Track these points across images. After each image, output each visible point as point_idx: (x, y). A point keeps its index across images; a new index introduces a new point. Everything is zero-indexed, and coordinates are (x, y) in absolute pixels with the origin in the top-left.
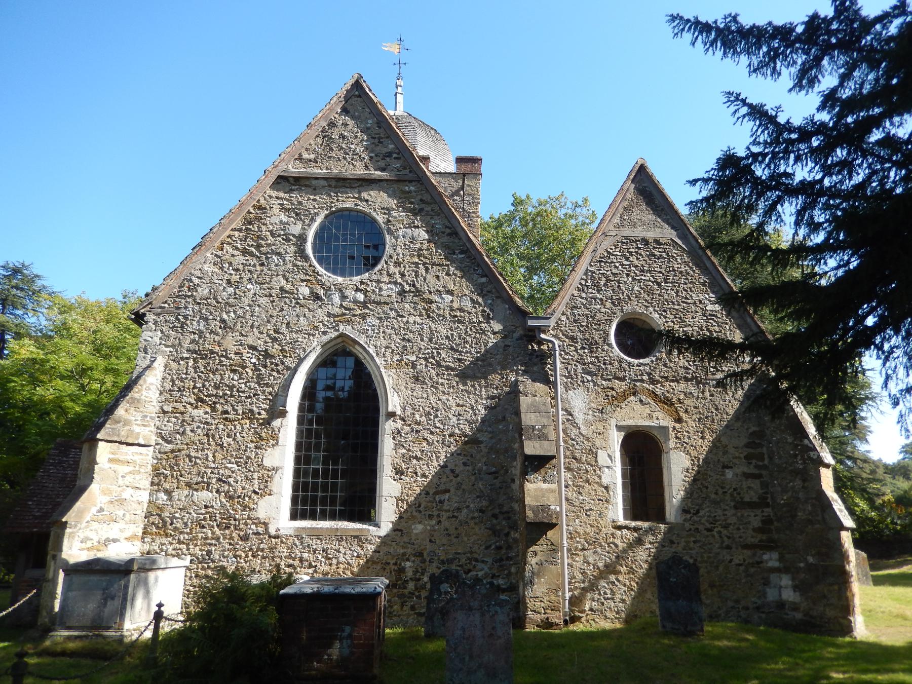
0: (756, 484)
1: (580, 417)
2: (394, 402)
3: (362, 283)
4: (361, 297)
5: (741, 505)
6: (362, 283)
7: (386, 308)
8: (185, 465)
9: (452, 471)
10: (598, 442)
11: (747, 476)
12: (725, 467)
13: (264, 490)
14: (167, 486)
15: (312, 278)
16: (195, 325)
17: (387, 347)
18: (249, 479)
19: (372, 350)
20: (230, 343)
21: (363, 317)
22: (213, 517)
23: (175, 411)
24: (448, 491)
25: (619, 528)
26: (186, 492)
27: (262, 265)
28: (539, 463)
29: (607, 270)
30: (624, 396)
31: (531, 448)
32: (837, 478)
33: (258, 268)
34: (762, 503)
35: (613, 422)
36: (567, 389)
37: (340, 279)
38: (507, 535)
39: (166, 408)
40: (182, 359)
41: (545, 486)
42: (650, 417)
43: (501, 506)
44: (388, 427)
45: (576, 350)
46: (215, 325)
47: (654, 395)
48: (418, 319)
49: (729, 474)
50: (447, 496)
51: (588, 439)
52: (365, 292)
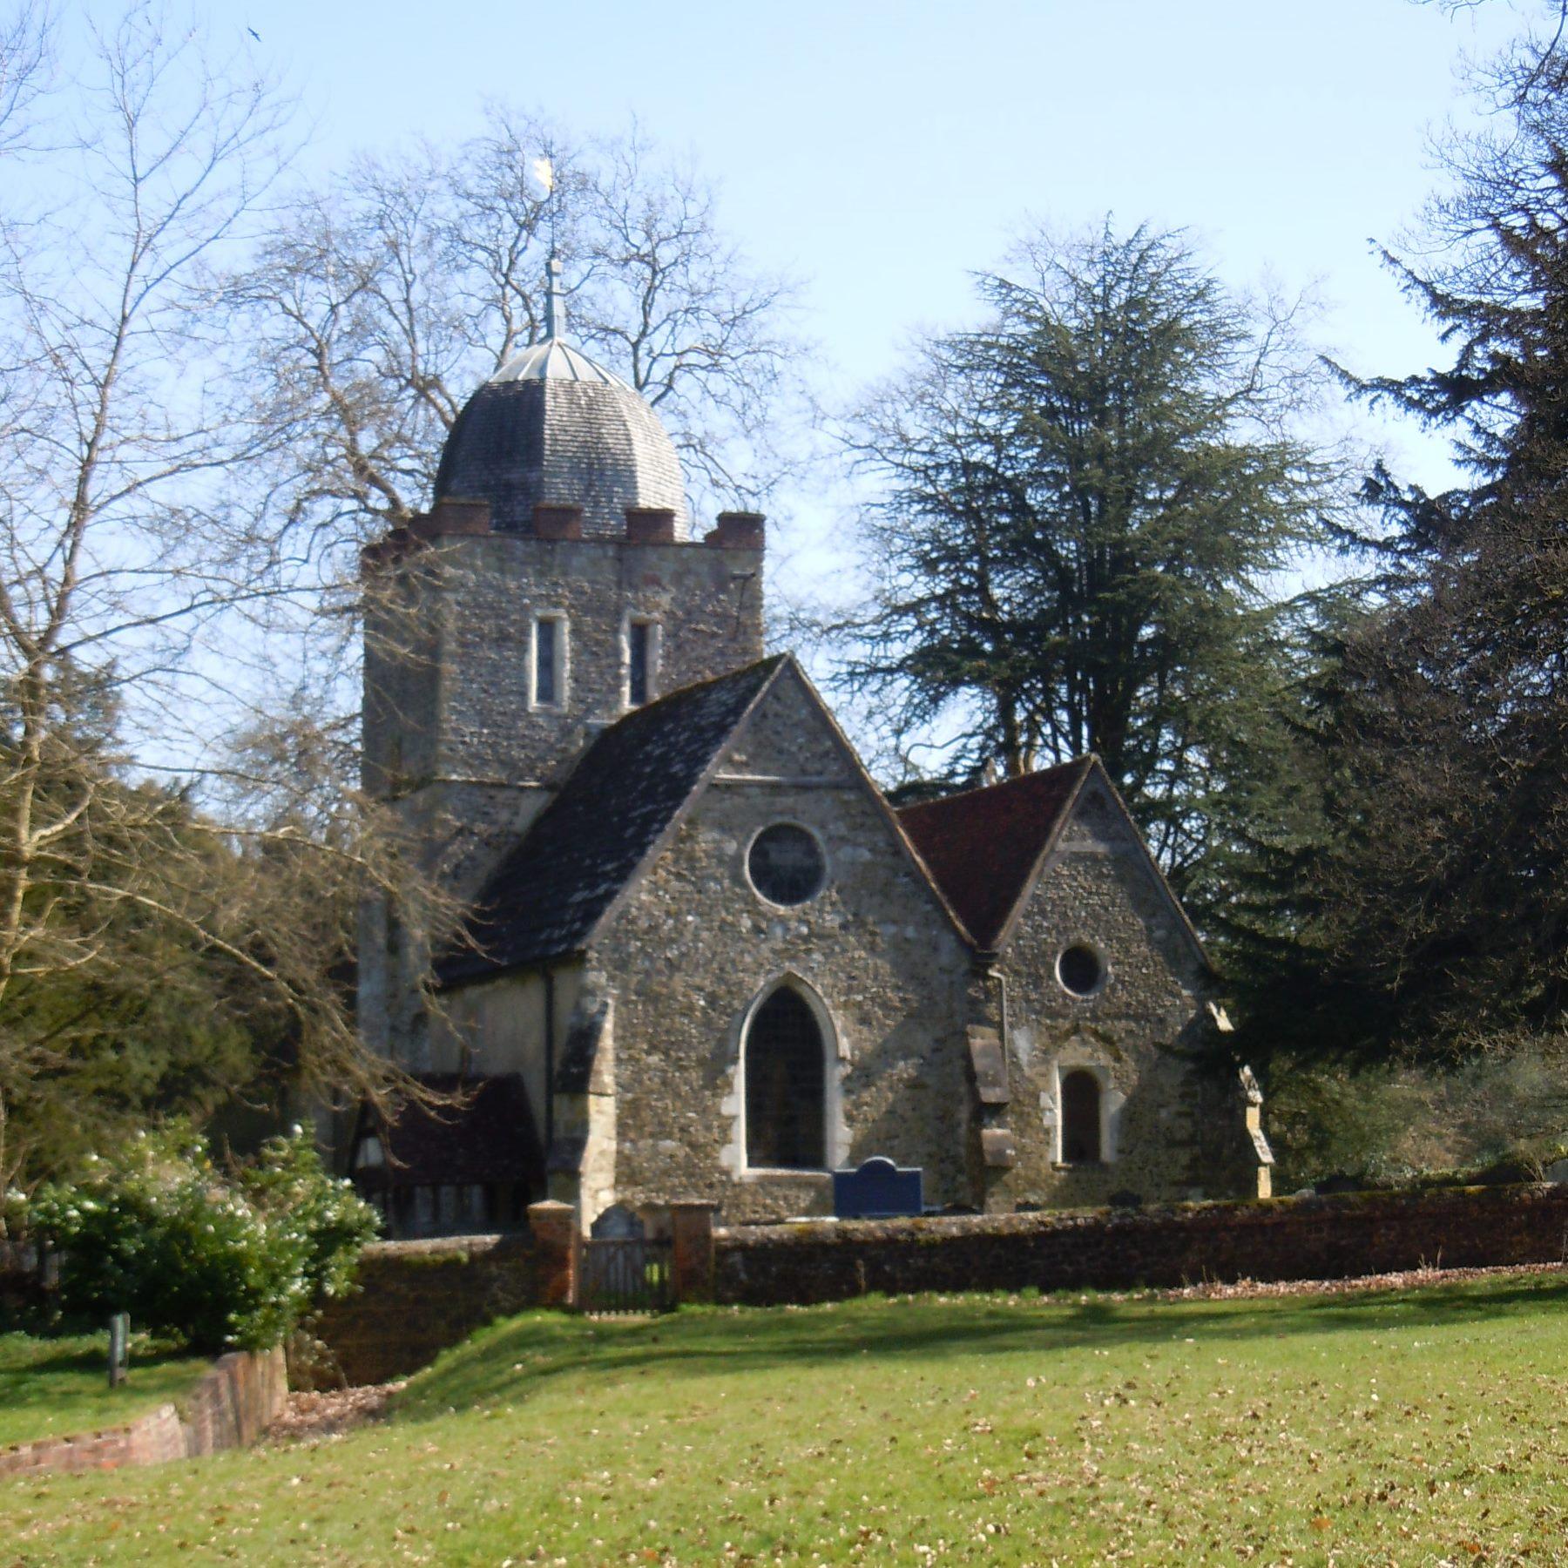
0: (1187, 1123)
1: (1024, 1057)
2: (845, 1046)
4: (805, 930)
5: (1172, 1143)
7: (830, 942)
8: (646, 1114)
9: (902, 1117)
10: (1041, 1082)
11: (1180, 1114)
12: (1161, 1106)
13: (725, 1139)
15: (753, 907)
16: (641, 964)
17: (834, 986)
18: (708, 1128)
19: (819, 989)
20: (678, 982)
21: (808, 952)
23: (631, 1058)
24: (897, 1137)
25: (1058, 1169)
26: (650, 1141)
27: (700, 892)
28: (996, 1110)
29: (1052, 894)
30: (1067, 1035)
31: (990, 1095)
32: (1265, 1113)
33: (696, 896)
34: (1190, 1142)
35: (1055, 1063)
36: (1012, 1026)
37: (782, 909)
38: (954, 1179)
41: (999, 1131)
42: (1091, 1057)
43: (947, 1151)
44: (835, 1075)
45: (1021, 986)
46: (661, 964)
47: (1095, 1033)
48: (863, 954)
49: (1163, 1114)
50: (896, 1142)
51: (1030, 1080)
52: (808, 923)
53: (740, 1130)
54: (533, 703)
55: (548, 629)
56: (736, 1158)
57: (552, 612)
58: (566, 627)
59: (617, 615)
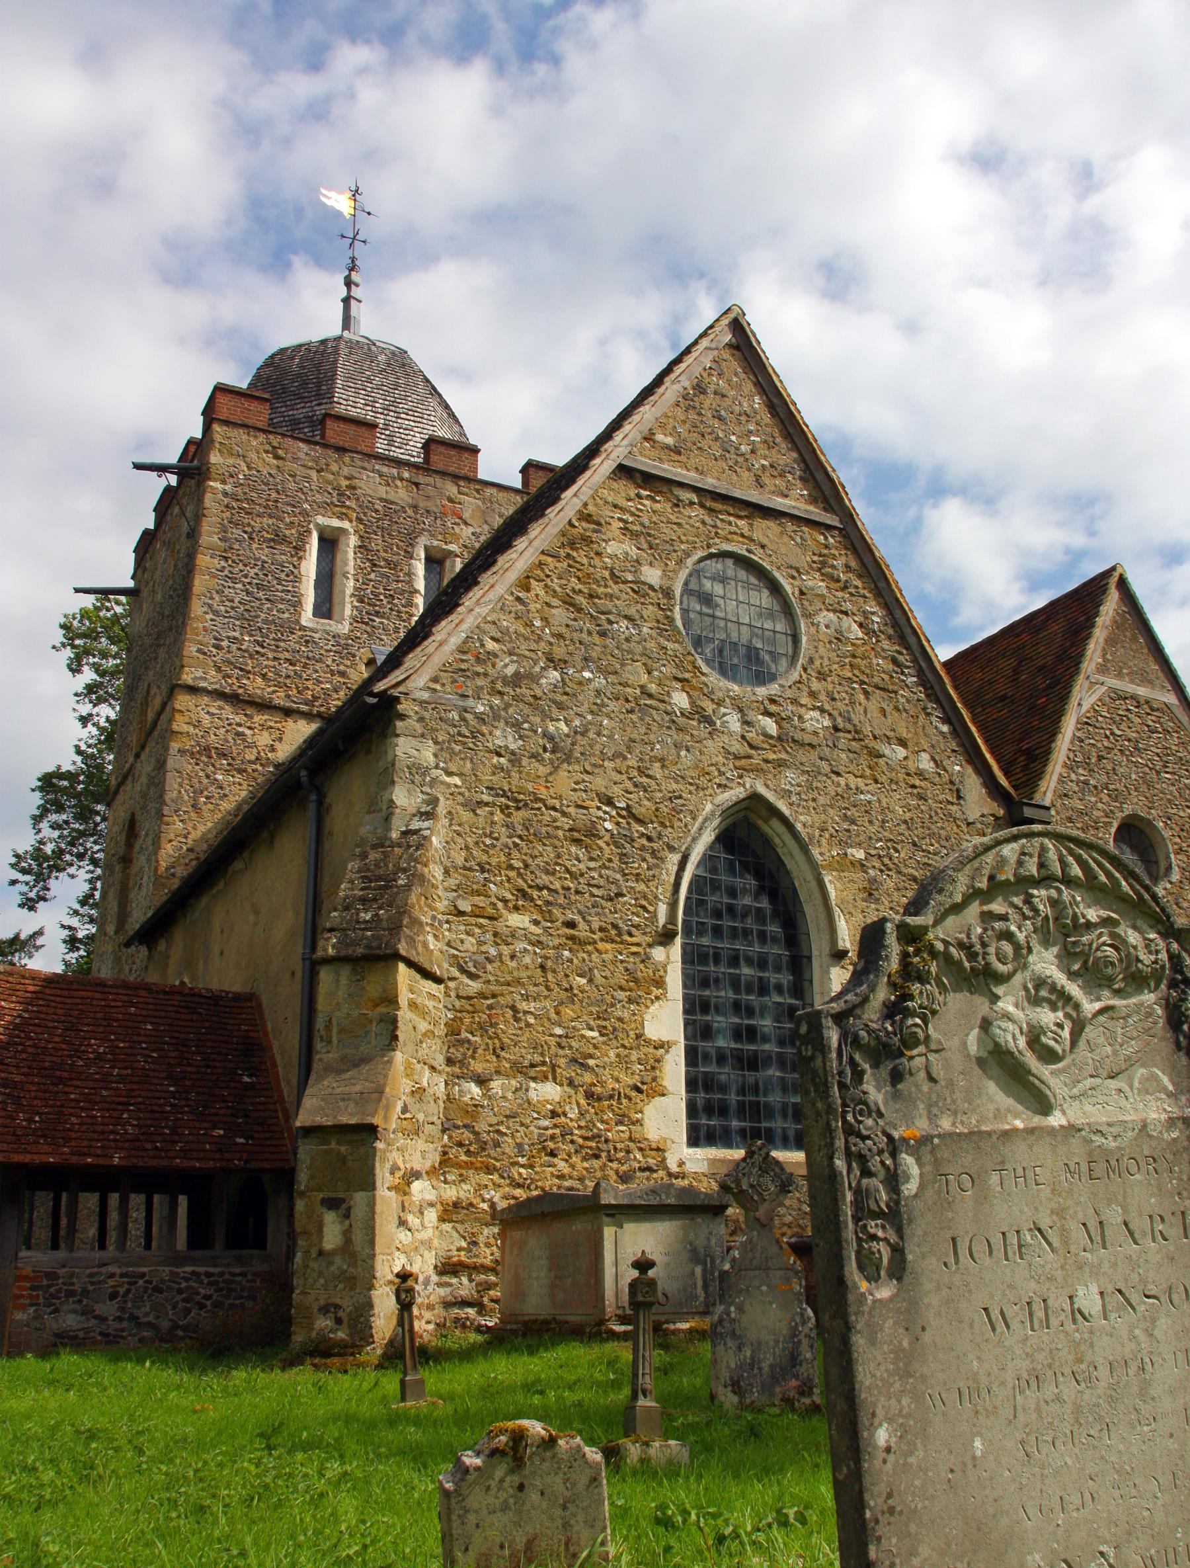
3: (773, 701)
6: (773, 701)
14: (478, 1067)
20: (564, 781)
22: (566, 1132)
39: (465, 906)
40: (481, 804)
53: (674, 1072)
54: (307, 616)
55: (330, 543)
56: (665, 1118)
57: (336, 523)
58: (353, 541)
59: (411, 539)
